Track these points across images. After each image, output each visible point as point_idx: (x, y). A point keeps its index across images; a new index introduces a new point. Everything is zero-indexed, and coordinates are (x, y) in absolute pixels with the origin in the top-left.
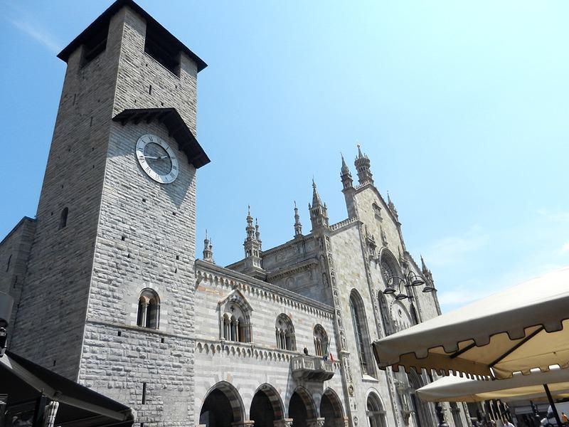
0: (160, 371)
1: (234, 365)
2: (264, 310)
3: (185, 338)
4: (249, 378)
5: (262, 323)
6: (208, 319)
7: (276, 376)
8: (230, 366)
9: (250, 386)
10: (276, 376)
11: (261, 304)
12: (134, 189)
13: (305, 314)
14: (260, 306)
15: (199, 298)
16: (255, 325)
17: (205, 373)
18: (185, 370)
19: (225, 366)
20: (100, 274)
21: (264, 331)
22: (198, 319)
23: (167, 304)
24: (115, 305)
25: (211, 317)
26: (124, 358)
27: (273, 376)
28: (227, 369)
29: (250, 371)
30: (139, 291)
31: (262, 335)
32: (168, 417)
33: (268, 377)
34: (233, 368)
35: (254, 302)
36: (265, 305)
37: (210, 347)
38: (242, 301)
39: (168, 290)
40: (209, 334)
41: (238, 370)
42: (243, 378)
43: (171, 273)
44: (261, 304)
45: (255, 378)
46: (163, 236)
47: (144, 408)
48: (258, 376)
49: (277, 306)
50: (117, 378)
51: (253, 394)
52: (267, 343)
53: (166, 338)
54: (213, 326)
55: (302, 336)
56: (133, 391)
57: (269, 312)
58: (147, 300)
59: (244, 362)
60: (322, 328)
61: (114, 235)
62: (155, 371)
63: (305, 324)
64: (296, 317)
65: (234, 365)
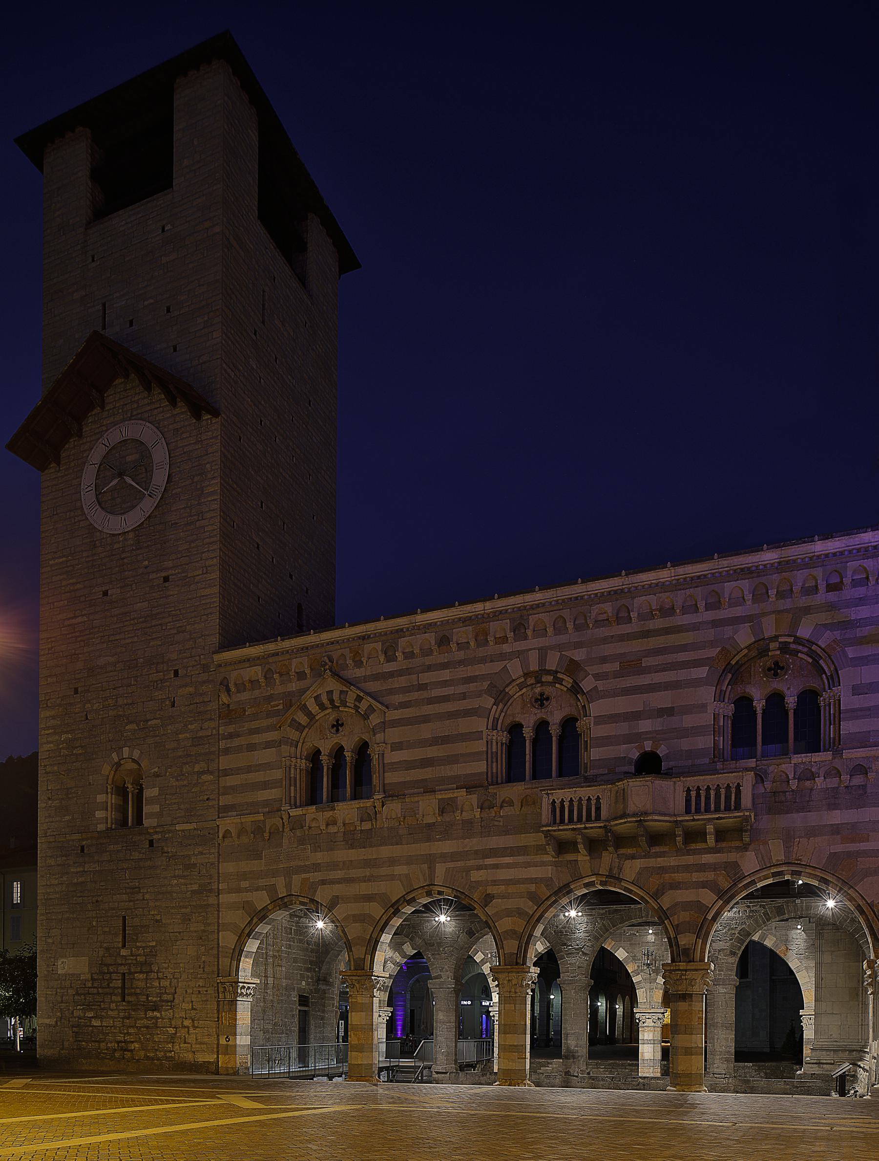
0: (147, 897)
2: (436, 692)
5: (426, 731)
6: (251, 776)
14: (422, 687)
15: (231, 736)
21: (432, 752)
22: (231, 781)
25: (260, 767)
31: (426, 763)
36: (446, 675)
47: (123, 952)
49: (502, 657)
54: (265, 785)
57: (461, 689)
62: (140, 896)
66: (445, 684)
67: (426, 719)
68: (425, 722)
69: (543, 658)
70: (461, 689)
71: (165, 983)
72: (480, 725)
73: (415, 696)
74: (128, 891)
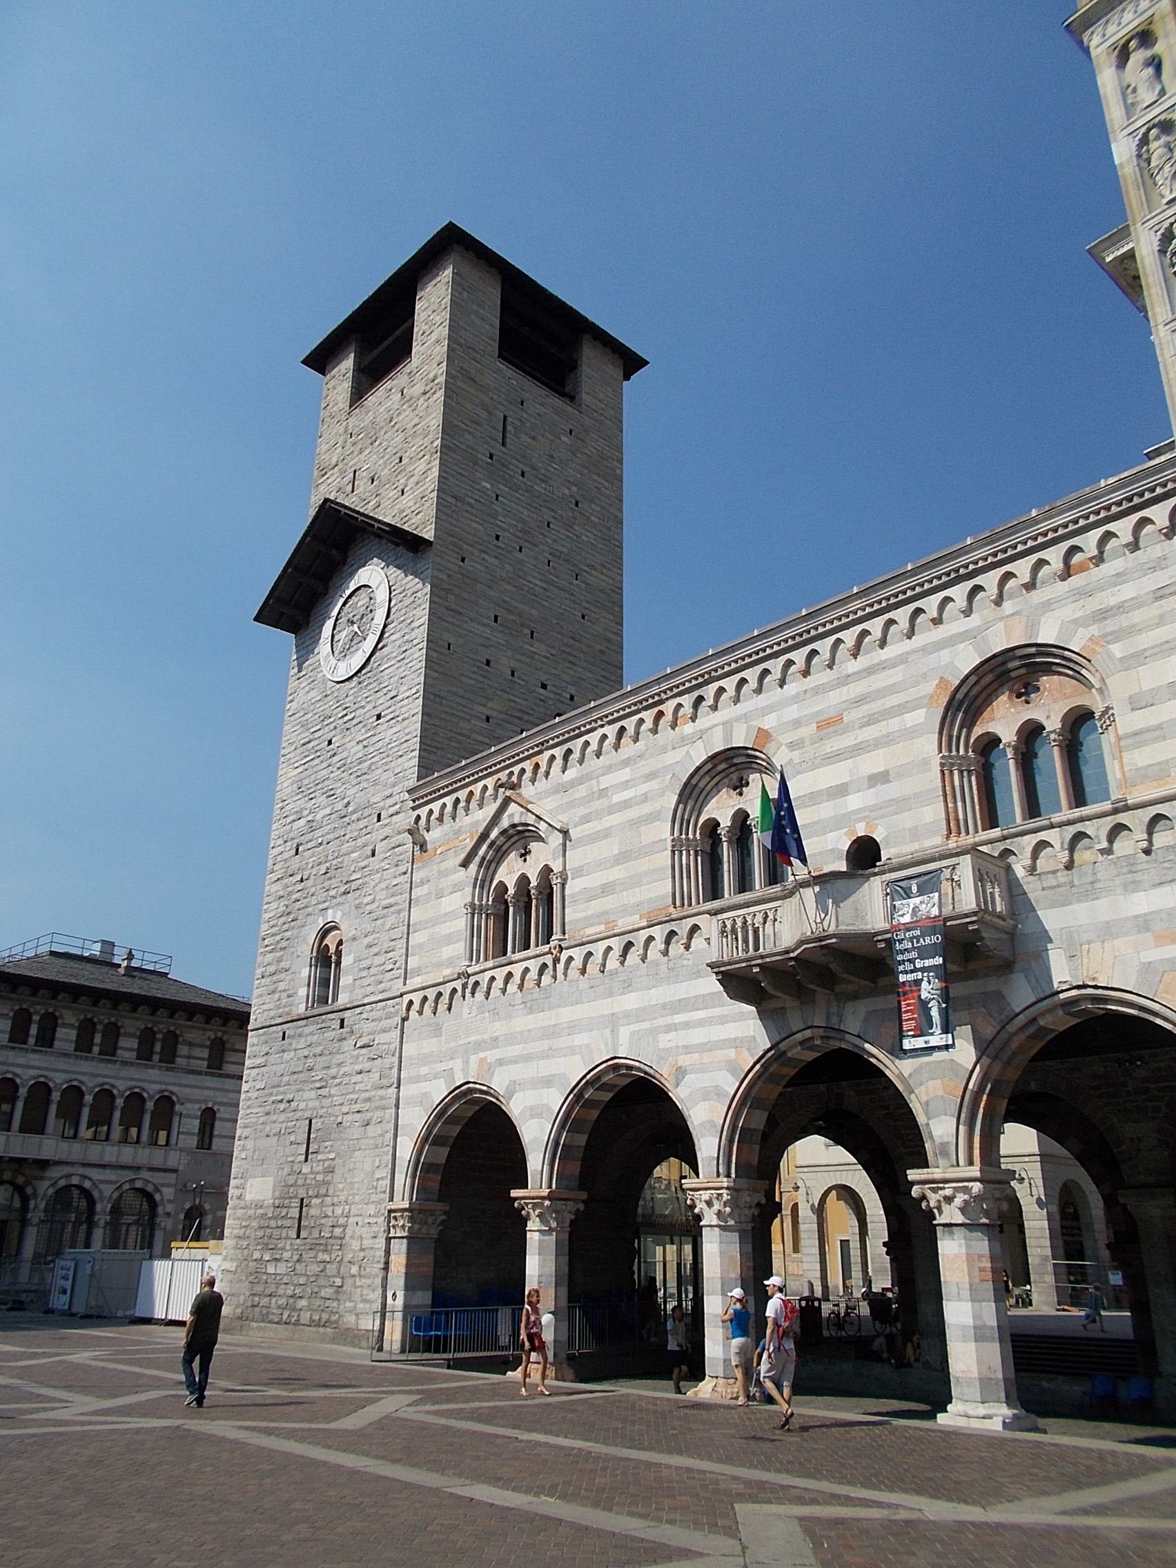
1: (499, 1028)
2: (617, 798)
3: (381, 1001)
4: (546, 1055)
7: (661, 1022)
8: (486, 1037)
9: (547, 1082)
10: (661, 1022)
11: (606, 781)
12: (317, 735)
13: (870, 671)
14: (603, 793)
16: (579, 872)
17: (424, 1070)
18: (377, 1076)
19: (472, 1039)
20: (266, 942)
23: (354, 939)
24: (282, 986)
26: (286, 1079)
27: (646, 1025)
28: (479, 1046)
29: (551, 1032)
30: (312, 936)
32: (341, 1186)
33: (624, 1033)
34: (496, 1039)
35: (581, 791)
36: (625, 774)
37: (441, 998)
38: (530, 819)
39: (357, 907)
40: (439, 965)
41: (511, 1039)
42: (527, 1058)
43: (363, 864)
44: (606, 781)
45: (572, 1050)
46: (354, 790)
47: (306, 1169)
48: (580, 1039)
49: (684, 741)
50: (275, 1117)
51: (555, 1100)
52: (625, 910)
53: (347, 1014)
55: (841, 790)
56: (292, 1138)
57: (643, 788)
58: (332, 949)
59: (531, 1011)
60: (1044, 649)
61: (286, 855)
63: (870, 721)
64: (797, 723)
65: (499, 1028)
66: (626, 785)
67: (606, 834)
68: (606, 837)
69: (728, 734)
70: (643, 788)
71: (339, 1211)
72: (663, 831)
73: (597, 805)
74: (318, 1085)
